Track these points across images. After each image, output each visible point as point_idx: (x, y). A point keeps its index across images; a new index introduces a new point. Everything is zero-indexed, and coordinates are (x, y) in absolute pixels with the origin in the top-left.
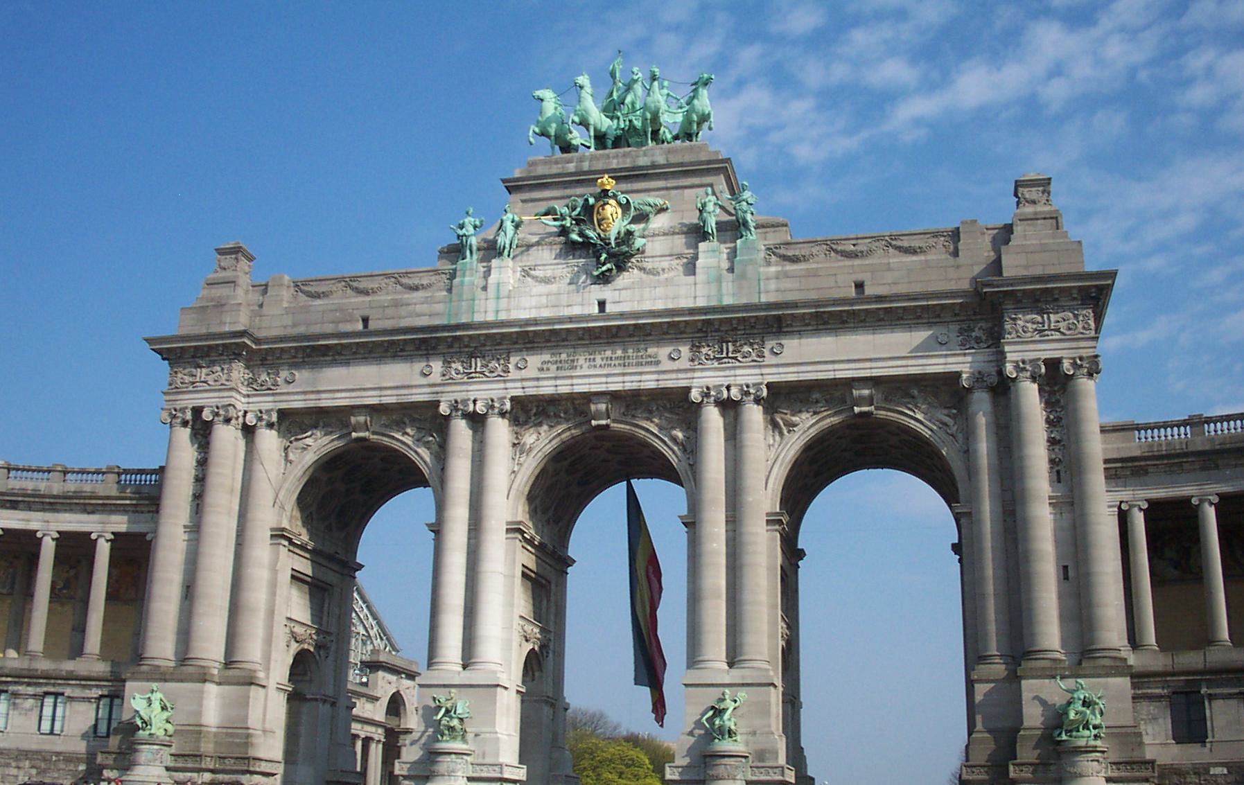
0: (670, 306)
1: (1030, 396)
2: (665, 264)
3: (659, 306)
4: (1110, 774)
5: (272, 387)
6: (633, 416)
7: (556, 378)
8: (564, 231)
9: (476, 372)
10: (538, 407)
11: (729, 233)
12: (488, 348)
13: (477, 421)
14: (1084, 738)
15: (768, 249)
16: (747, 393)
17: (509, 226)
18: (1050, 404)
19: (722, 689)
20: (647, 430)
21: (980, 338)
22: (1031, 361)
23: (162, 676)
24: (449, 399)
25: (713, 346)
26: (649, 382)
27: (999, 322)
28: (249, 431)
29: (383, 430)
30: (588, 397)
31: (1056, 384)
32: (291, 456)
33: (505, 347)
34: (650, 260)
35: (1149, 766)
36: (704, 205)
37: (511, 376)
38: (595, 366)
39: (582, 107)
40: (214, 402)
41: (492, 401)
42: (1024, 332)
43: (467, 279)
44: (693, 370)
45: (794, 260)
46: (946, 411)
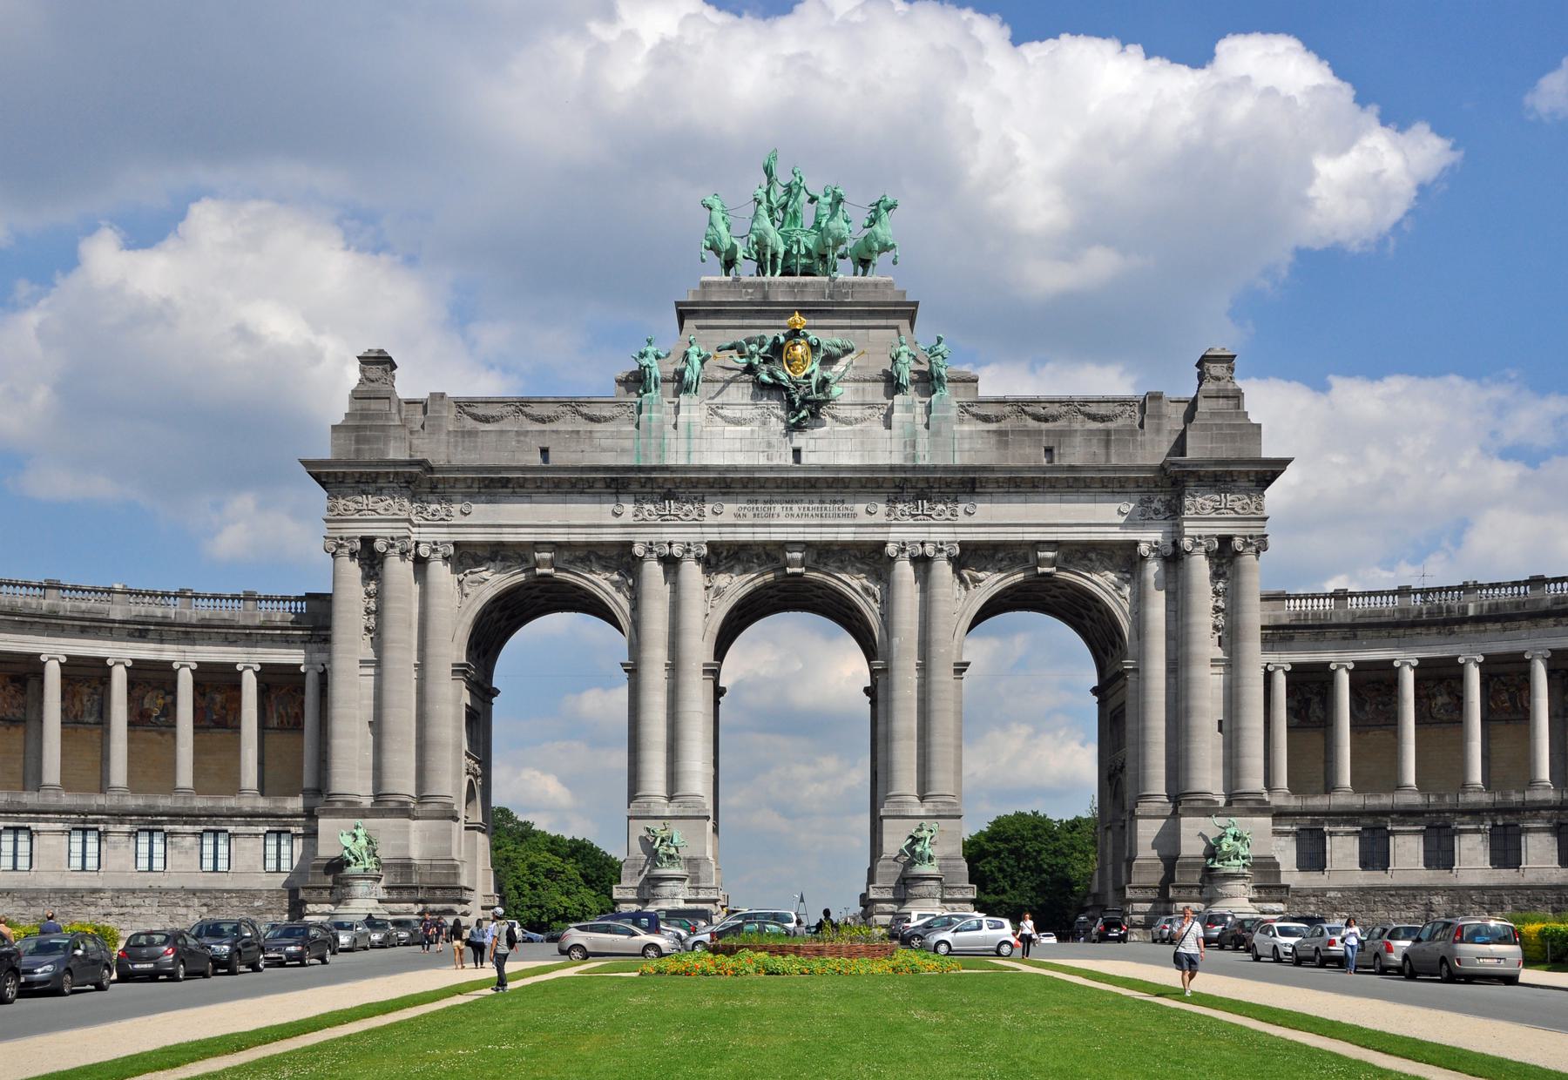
0: (867, 462)
1: (1200, 568)
2: (857, 413)
3: (855, 460)
4: (1251, 896)
5: (446, 518)
6: (825, 564)
7: (753, 526)
8: (750, 369)
9: (670, 515)
10: (728, 551)
11: (920, 385)
12: (681, 490)
13: (671, 564)
14: (1234, 866)
15: (962, 406)
16: (941, 551)
17: (696, 360)
18: (1216, 576)
19: (920, 821)
20: (839, 579)
21: (1158, 510)
22: (1207, 537)
23: (352, 810)
24: (644, 540)
25: (909, 502)
26: (846, 535)
27: (1180, 497)
28: (421, 563)
29: (567, 566)
30: (783, 546)
31: (1224, 557)
32: (467, 590)
33: (700, 490)
34: (841, 407)
35: (1285, 890)
36: (898, 355)
37: (708, 520)
38: (792, 515)
39: (761, 227)
40: (388, 533)
41: (689, 545)
42: (1203, 509)
43: (654, 415)
44: (889, 526)
45: (986, 419)
46: (1120, 575)
